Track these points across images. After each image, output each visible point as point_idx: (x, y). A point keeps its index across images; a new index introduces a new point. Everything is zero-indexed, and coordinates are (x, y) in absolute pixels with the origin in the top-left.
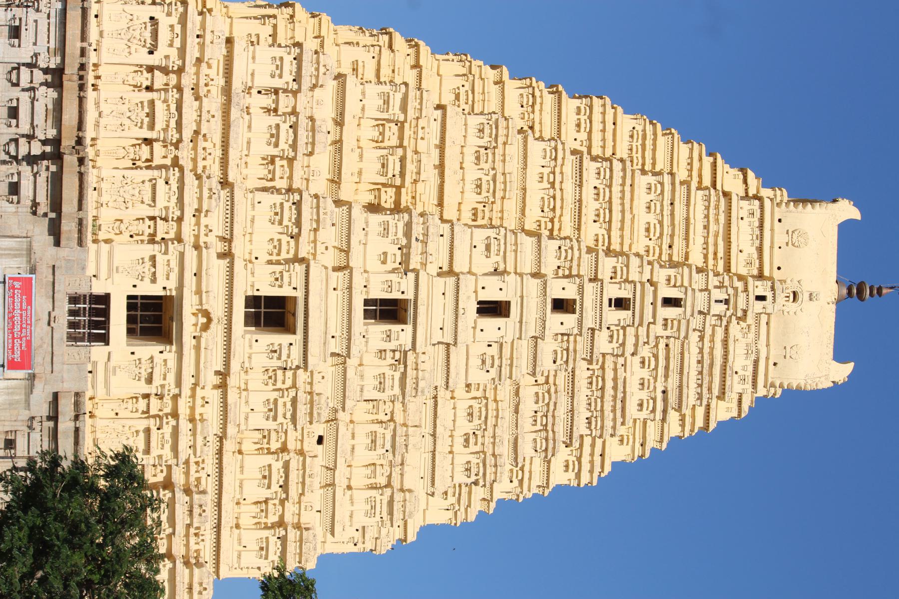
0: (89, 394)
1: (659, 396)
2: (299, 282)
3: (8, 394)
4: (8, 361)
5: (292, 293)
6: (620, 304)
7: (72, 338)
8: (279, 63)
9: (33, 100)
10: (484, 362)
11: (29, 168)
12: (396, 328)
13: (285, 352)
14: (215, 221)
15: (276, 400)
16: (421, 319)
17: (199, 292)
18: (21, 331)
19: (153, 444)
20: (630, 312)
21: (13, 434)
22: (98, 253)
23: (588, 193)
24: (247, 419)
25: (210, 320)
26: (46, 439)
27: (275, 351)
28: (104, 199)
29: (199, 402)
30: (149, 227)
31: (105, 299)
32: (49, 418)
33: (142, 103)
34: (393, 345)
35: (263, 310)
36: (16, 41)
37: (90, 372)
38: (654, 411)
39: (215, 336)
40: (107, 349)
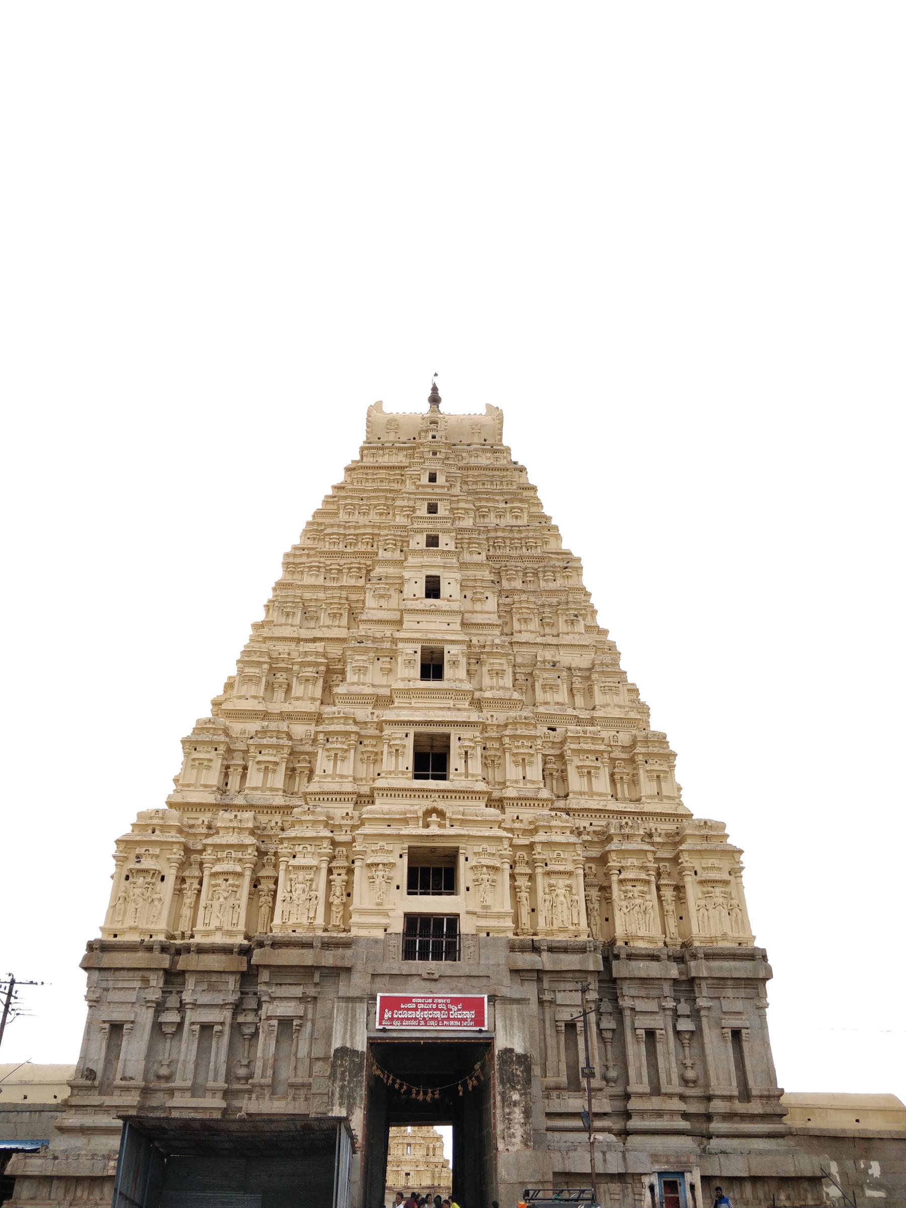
0: (511, 935)
1: (508, 505)
2: (399, 732)
3: (512, 1026)
4: (475, 1025)
6: (433, 509)
7: (452, 952)
8: (197, 763)
9: (195, 1006)
10: (479, 600)
11: (265, 1006)
12: (446, 657)
13: (467, 743)
14: (339, 810)
15: (514, 755)
16: (439, 636)
17: (406, 821)
18: (441, 1010)
20: (439, 503)
21: (558, 1024)
22: (361, 926)
23: (348, 550)
24: (533, 782)
25: (434, 810)
26: (562, 986)
27: (466, 753)
28: (305, 921)
29: (517, 825)
30: (339, 875)
31: (411, 919)
32: (540, 980)
33: (214, 886)
34: (463, 661)
35: (430, 773)
36: (125, 1026)
37: (488, 934)
38: (521, 509)
39: (450, 807)
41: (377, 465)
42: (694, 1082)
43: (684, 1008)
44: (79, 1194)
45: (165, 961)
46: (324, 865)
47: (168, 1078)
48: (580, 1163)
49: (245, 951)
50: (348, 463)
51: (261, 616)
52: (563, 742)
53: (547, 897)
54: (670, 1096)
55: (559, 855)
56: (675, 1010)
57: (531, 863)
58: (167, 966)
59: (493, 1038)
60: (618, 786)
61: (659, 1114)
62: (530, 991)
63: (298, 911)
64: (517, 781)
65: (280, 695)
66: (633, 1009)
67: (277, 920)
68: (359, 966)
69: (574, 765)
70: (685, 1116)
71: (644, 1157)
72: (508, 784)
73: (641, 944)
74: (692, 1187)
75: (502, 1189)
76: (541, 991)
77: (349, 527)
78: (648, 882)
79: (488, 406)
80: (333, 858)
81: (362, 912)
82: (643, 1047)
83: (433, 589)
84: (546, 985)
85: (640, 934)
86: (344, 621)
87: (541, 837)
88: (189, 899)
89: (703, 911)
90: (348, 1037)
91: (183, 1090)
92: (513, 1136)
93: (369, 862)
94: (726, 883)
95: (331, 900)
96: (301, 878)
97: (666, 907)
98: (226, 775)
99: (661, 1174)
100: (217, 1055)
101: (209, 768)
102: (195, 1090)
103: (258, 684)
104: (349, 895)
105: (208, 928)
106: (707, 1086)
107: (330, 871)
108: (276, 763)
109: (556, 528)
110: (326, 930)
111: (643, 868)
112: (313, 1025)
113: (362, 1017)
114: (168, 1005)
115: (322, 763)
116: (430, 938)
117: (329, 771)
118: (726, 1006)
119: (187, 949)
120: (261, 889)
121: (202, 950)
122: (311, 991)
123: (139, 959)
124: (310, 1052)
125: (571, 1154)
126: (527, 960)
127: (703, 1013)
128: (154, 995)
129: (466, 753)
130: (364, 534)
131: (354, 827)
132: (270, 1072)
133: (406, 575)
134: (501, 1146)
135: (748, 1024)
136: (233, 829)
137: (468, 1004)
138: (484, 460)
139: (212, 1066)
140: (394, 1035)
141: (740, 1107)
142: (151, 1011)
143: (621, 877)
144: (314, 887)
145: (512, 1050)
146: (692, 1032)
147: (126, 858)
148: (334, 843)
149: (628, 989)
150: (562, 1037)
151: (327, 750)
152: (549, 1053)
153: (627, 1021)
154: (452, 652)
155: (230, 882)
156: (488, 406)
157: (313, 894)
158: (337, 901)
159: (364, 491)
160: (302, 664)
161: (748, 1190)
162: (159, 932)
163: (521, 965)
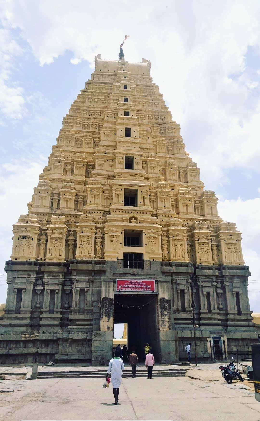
0: (162, 261)
3: (164, 291)
5: (123, 190)
7: (141, 266)
8: (40, 198)
11: (75, 284)
12: (134, 160)
14: (98, 216)
16: (132, 152)
17: (123, 221)
19: (179, 238)
24: (168, 208)
25: (133, 217)
26: (180, 277)
29: (162, 223)
31: (126, 254)
32: (172, 275)
40: (144, 254)
41: (100, 82)
42: (222, 309)
43: (219, 285)
44: (12, 346)
45: (37, 268)
46: (94, 235)
47: (40, 308)
48: (187, 334)
49: (66, 265)
50: (87, 81)
51: (55, 143)
52: (177, 195)
53: (174, 248)
54: (214, 313)
55: (178, 233)
56: (216, 286)
57: (168, 237)
58: (37, 270)
59: (157, 294)
60: (197, 210)
61: (210, 319)
62: (169, 279)
63: (85, 251)
64: (162, 208)
65: (69, 173)
66: (202, 286)
67: (77, 254)
68: (109, 270)
69: (181, 202)
70: (219, 320)
71: (208, 332)
72: (159, 208)
73: (205, 264)
74: (224, 342)
75: (162, 342)
76: (172, 280)
77: (91, 108)
78: (208, 243)
79: (143, 58)
80: (96, 233)
81: (109, 252)
82: (206, 298)
83: (128, 133)
84: (174, 277)
85: (206, 261)
86: (92, 145)
87: (171, 227)
88: (43, 246)
89: (227, 253)
90: (107, 293)
91: (45, 311)
92: (165, 326)
93: (111, 234)
94: (235, 244)
95: (96, 247)
96: (85, 240)
97: (214, 252)
98: (52, 203)
99: (213, 338)
100: (57, 300)
101: (46, 199)
102: (51, 311)
103: (61, 168)
104: (102, 246)
105: (51, 257)
106: (227, 310)
107: (95, 238)
108: (71, 199)
109: (170, 112)
110: (95, 258)
111: (207, 239)
112: (92, 290)
113: (112, 287)
114: (38, 283)
115: (89, 199)
116: (133, 261)
117: (93, 202)
118: (234, 285)
119: (44, 264)
120: (71, 244)
121: (50, 264)
122: (92, 279)
123: (26, 267)
124: (91, 299)
125: (184, 331)
126: (167, 269)
127: (226, 287)
128: (33, 280)
129: (144, 197)
130: (97, 110)
131: (103, 223)
132: (78, 305)
133: (118, 127)
134: (161, 329)
135: (241, 291)
136: (58, 223)
137: (148, 283)
138: (143, 82)
139: (56, 304)
140: (123, 293)
141: (238, 317)
142: (32, 285)
143: (199, 241)
144: (90, 243)
145: (164, 298)
146: (222, 293)
147: (18, 231)
148: (97, 228)
149: (201, 279)
150: (179, 295)
151: (91, 194)
152: (175, 299)
153: (200, 289)
154: (137, 159)
155: (58, 241)
156: (143, 58)
157: (90, 245)
158: (99, 248)
159: (96, 92)
160: (77, 162)
161: (241, 342)
162: (33, 258)
163: (165, 270)
